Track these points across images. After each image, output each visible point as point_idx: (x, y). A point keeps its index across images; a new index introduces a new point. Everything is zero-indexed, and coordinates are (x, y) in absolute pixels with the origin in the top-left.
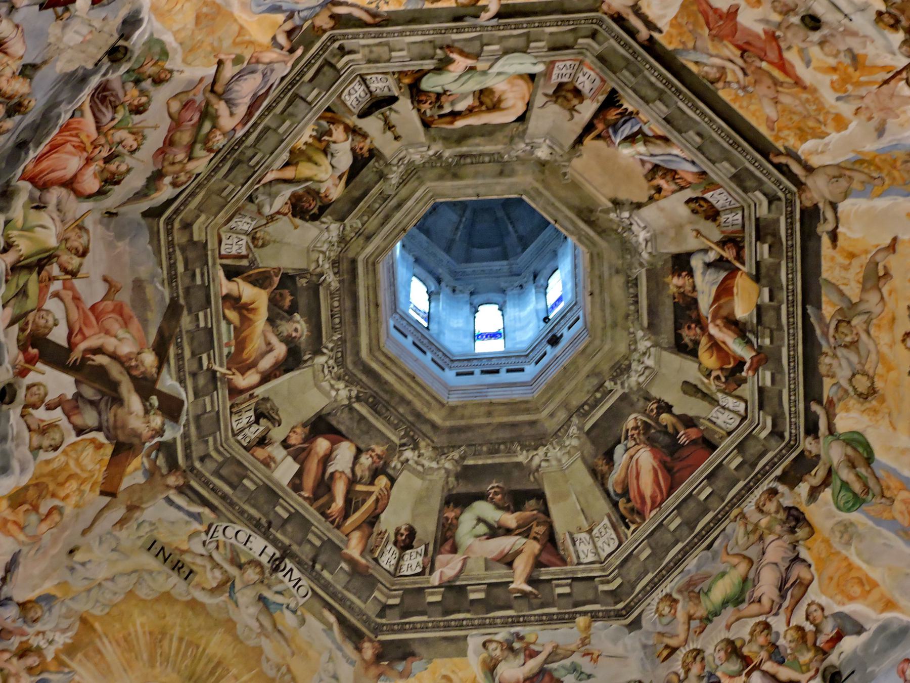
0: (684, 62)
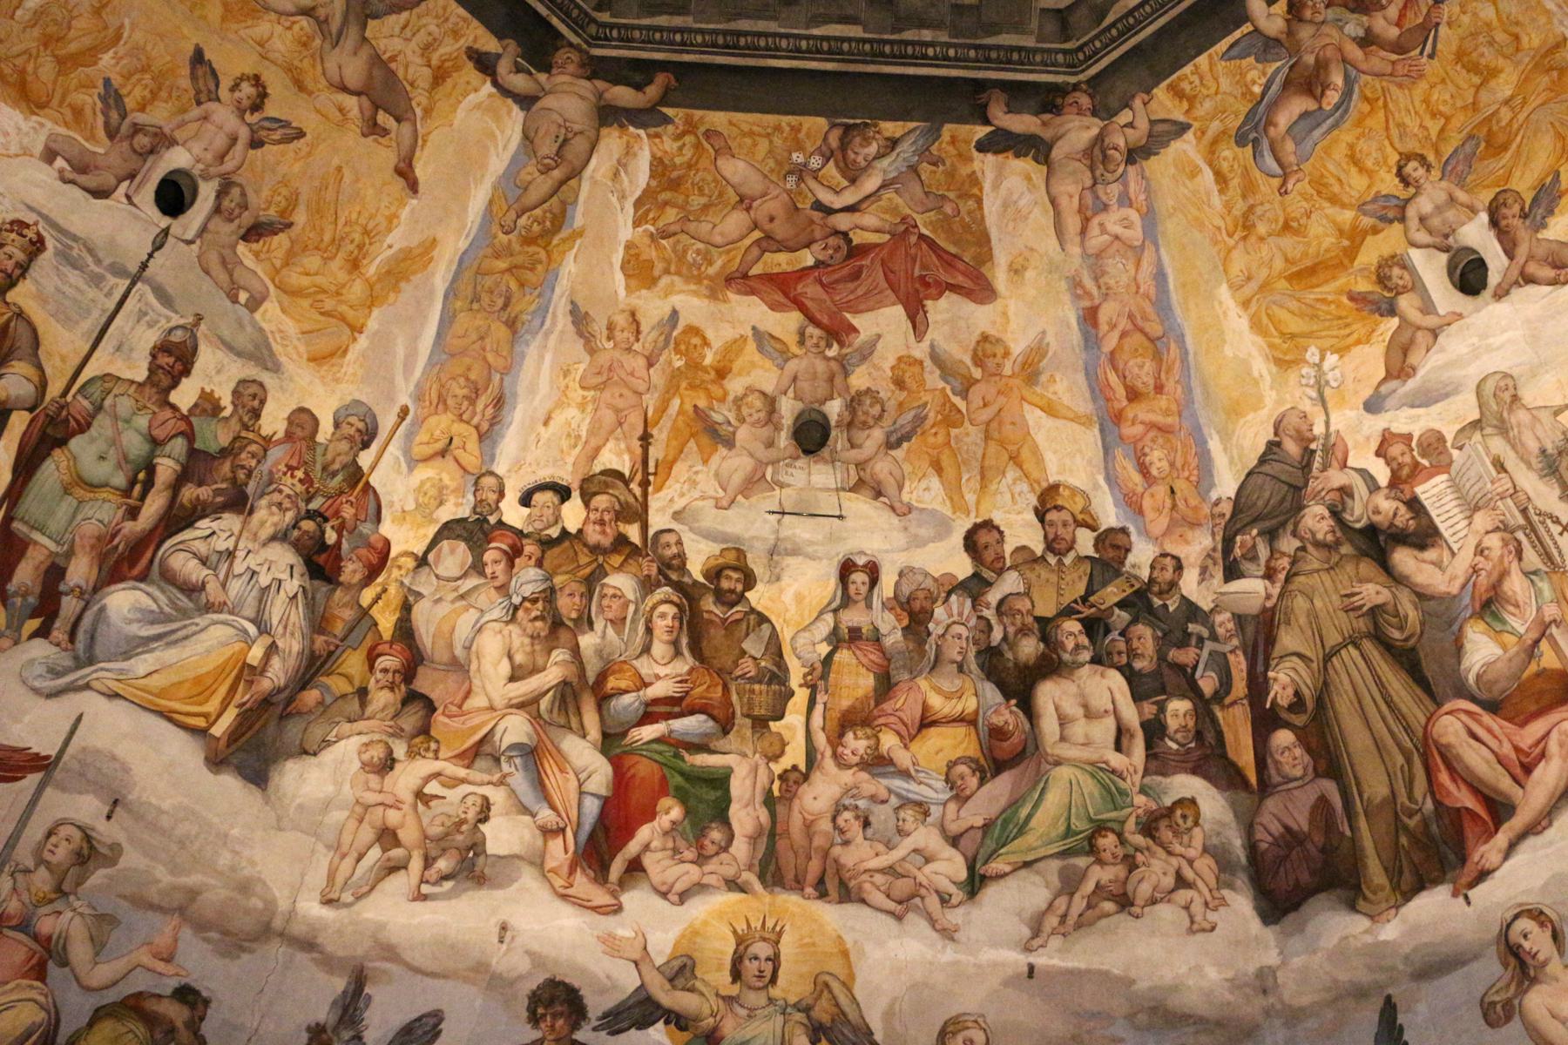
0: (914, 124)
